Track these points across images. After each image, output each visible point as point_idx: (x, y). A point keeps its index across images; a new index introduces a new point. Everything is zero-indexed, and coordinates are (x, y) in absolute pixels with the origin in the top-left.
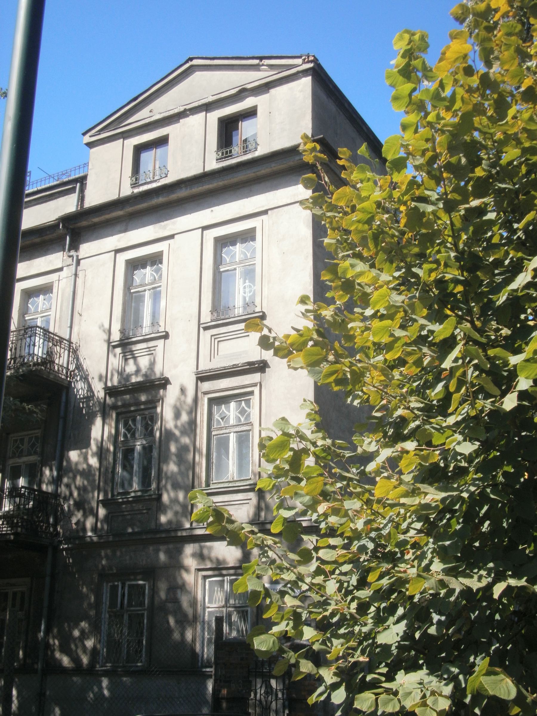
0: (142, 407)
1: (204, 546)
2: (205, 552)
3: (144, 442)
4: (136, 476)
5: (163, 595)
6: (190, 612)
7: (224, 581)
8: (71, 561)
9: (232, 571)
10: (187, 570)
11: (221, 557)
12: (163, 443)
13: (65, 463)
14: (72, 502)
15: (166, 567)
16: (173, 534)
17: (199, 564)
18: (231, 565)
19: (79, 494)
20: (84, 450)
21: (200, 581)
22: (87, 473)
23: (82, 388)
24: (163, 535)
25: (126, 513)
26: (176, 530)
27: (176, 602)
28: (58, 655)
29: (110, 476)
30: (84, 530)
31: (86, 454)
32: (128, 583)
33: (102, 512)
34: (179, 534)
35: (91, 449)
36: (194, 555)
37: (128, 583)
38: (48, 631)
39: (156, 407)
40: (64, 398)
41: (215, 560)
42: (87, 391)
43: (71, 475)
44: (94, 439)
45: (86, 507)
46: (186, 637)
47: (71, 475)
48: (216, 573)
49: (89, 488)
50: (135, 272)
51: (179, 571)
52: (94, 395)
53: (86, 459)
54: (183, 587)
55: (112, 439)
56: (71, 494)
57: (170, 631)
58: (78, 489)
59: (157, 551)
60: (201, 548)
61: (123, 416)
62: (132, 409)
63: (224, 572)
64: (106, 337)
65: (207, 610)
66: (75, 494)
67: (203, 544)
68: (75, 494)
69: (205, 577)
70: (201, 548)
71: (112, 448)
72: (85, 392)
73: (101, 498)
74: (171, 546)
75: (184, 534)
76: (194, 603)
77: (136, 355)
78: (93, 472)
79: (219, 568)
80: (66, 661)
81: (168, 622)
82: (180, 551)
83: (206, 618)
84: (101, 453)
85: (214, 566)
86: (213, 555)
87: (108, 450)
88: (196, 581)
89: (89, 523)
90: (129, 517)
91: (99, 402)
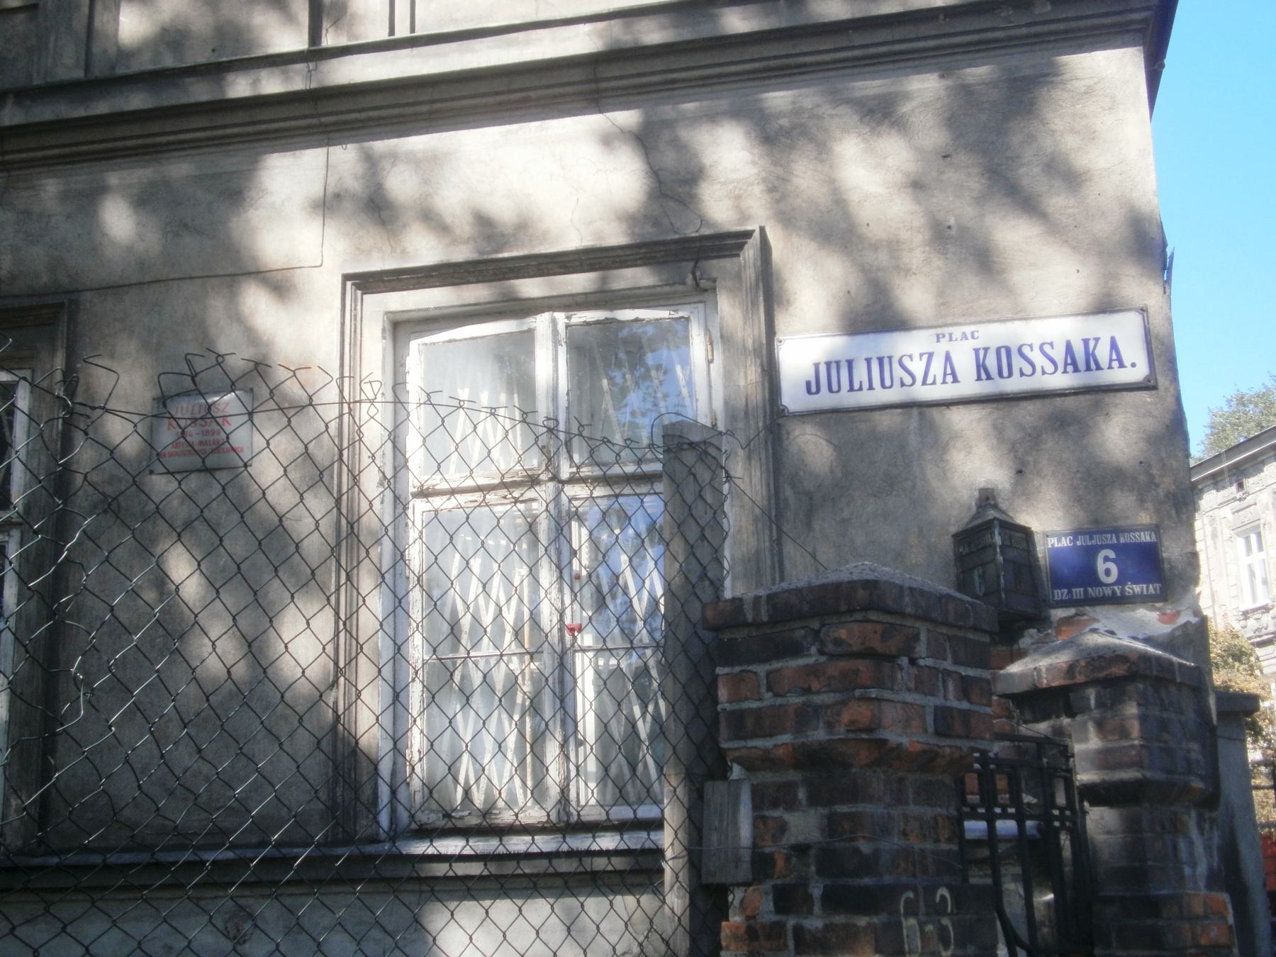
1: (394, 157)
2: (400, 185)
5: (120, 431)
6: (310, 518)
7: (527, 337)
9: (579, 282)
10: (280, 285)
11: (502, 210)
15: (143, 283)
16: (200, 92)
17: (361, 252)
18: (572, 241)
21: (374, 345)
24: (137, 101)
26: (217, 70)
27: (214, 463)
34: (240, 87)
36: (328, 205)
41: (464, 227)
46: (288, 669)
48: (476, 293)
51: (233, 296)
54: (255, 379)
57: (173, 629)
59: (94, 195)
60: (372, 163)
63: (531, 288)
65: (419, 509)
67: (380, 146)
69: (402, 328)
70: (372, 163)
74: (180, 169)
75: (272, 84)
76: (325, 471)
79: (496, 270)
81: (161, 579)
82: (235, 192)
83: (416, 556)
85: (461, 254)
86: (452, 200)
88: (349, 341)
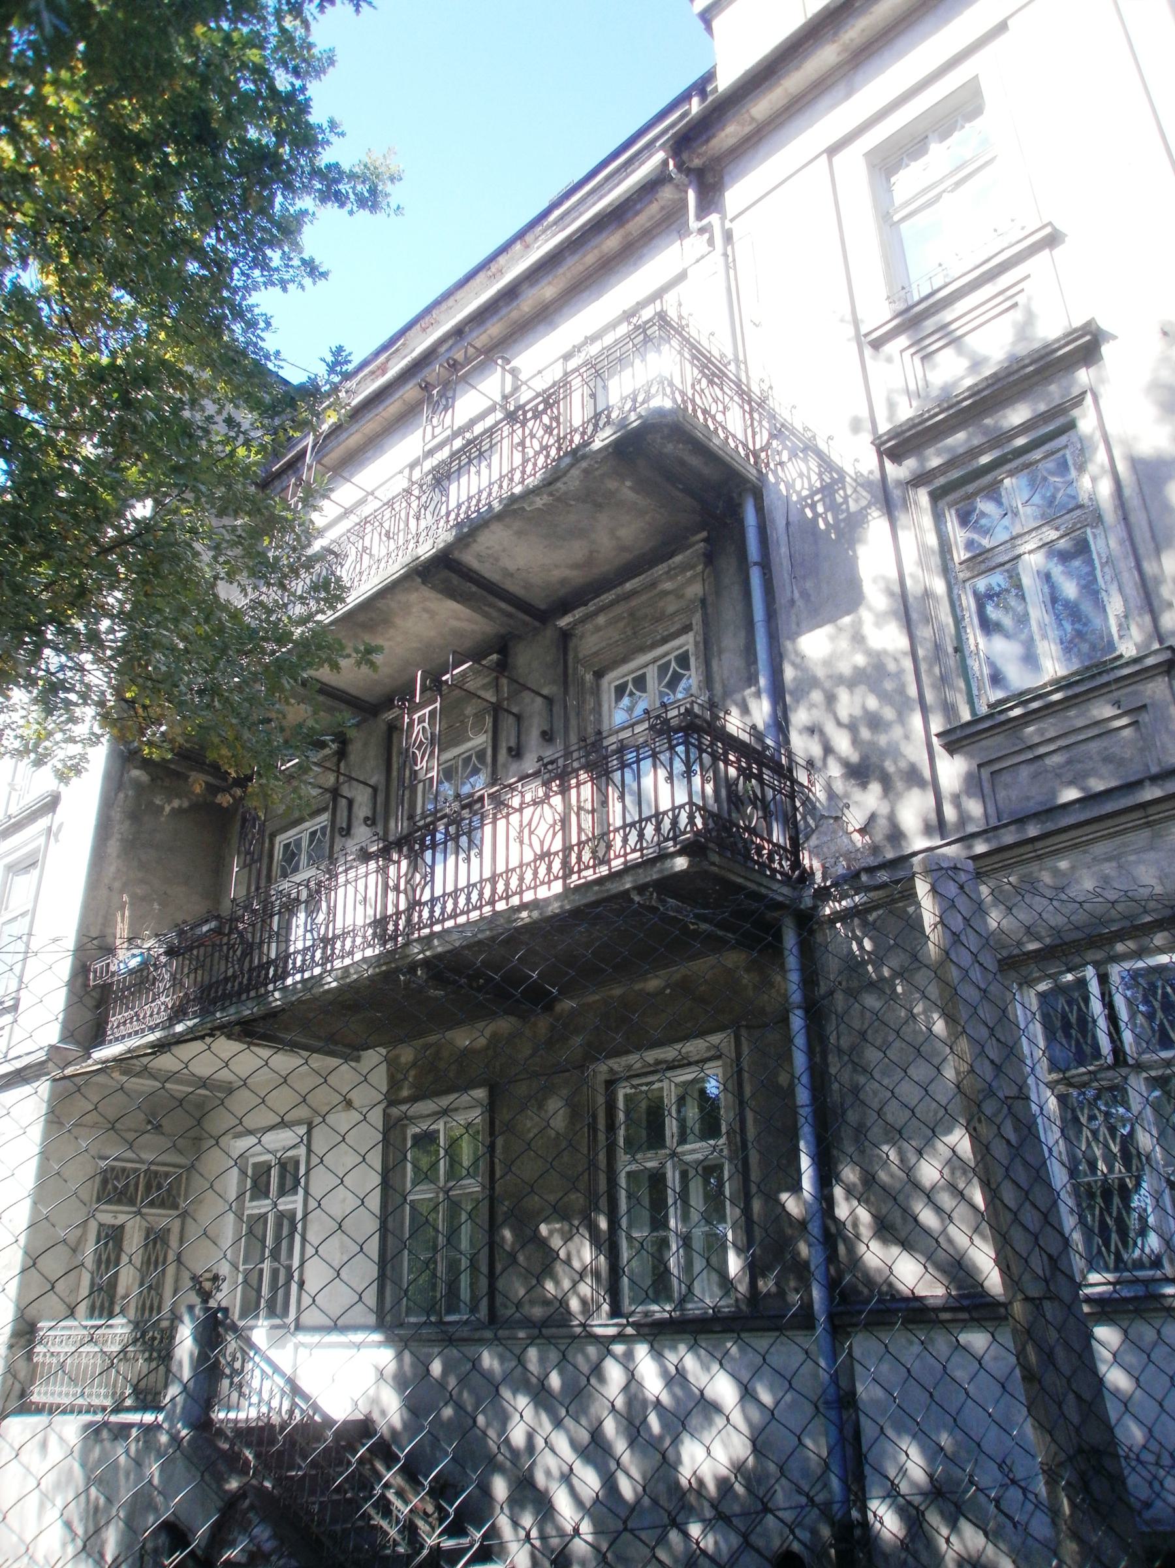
0: (1020, 441)
3: (1053, 535)
4: (1044, 636)
8: (868, 945)
12: (1134, 502)
13: (789, 673)
14: (835, 770)
19: (856, 741)
20: (847, 620)
22: (873, 675)
23: (801, 475)
25: (1042, 750)
28: (875, 1254)
29: (952, 661)
30: (896, 835)
31: (857, 625)
32: (1116, 972)
33: (952, 771)
35: (870, 609)
37: (1116, 972)
38: (826, 1177)
39: (1071, 426)
40: (751, 518)
42: (820, 475)
43: (817, 696)
44: (875, 581)
45: (890, 767)
47: (817, 696)
49: (889, 713)
50: (893, 180)
52: (841, 473)
53: (858, 639)
55: (935, 561)
56: (828, 750)
58: (852, 727)
61: (950, 498)
62: (985, 459)
64: (851, 332)
66: (842, 743)
68: (842, 743)
71: (939, 586)
72: (814, 477)
73: (937, 726)
77: (959, 333)
78: (891, 667)
80: (909, 1273)
84: (908, 610)
87: (927, 594)
89: (912, 812)
90: (1057, 759)
91: (867, 485)
